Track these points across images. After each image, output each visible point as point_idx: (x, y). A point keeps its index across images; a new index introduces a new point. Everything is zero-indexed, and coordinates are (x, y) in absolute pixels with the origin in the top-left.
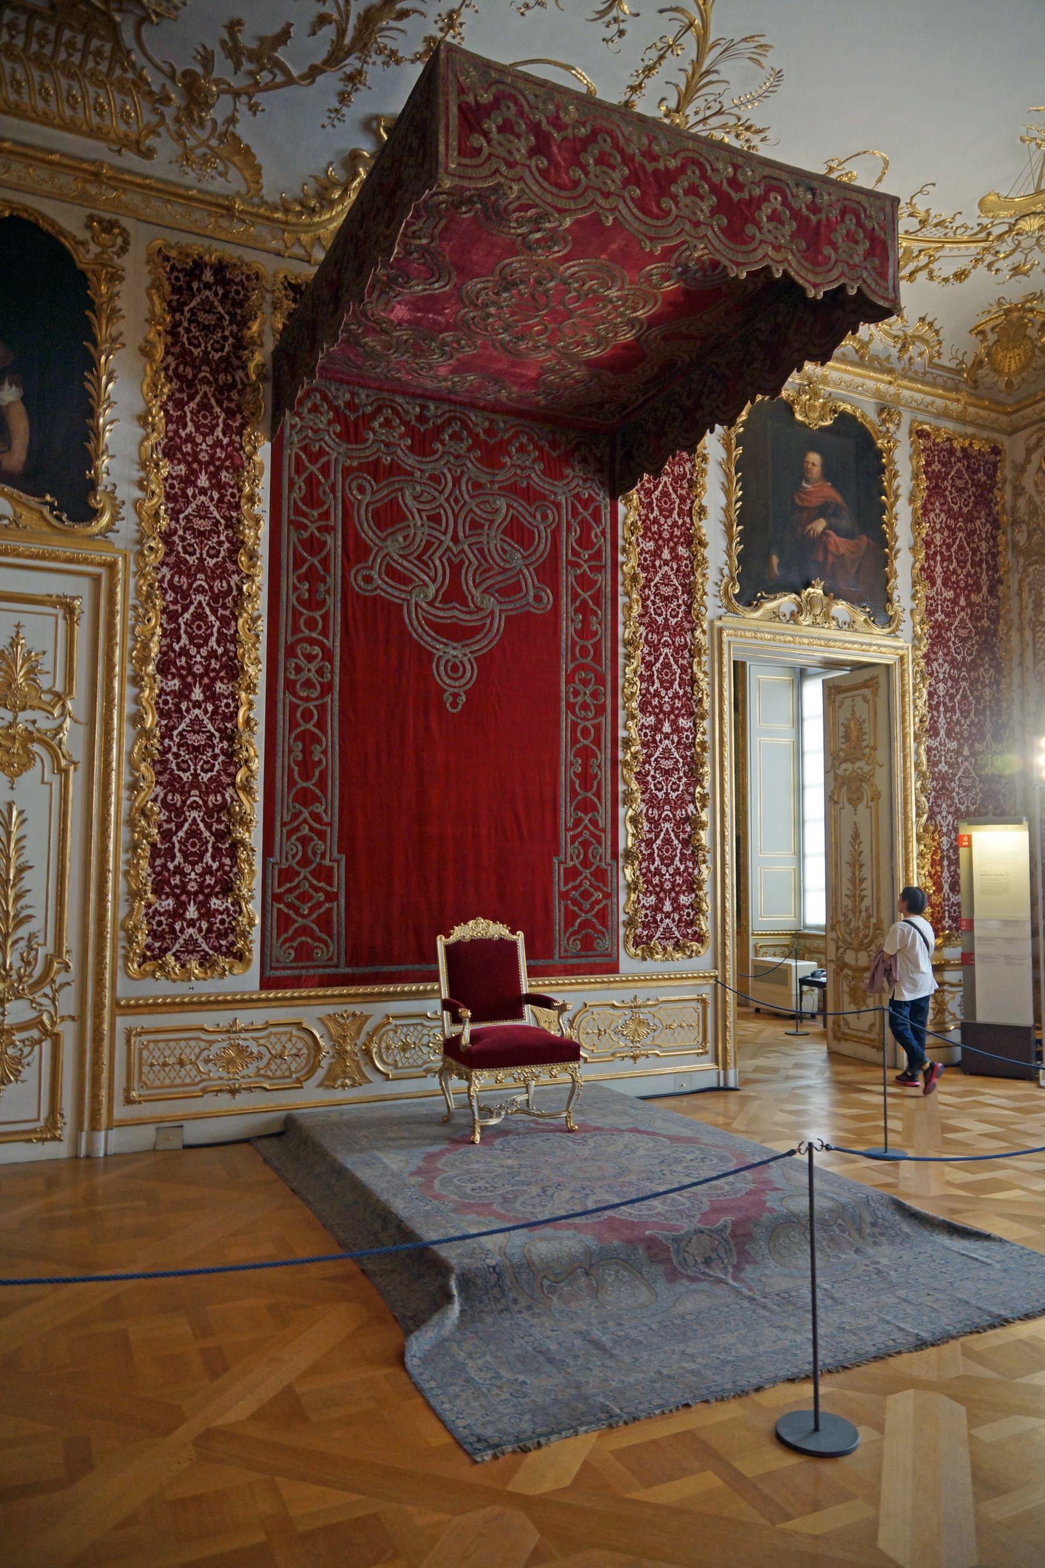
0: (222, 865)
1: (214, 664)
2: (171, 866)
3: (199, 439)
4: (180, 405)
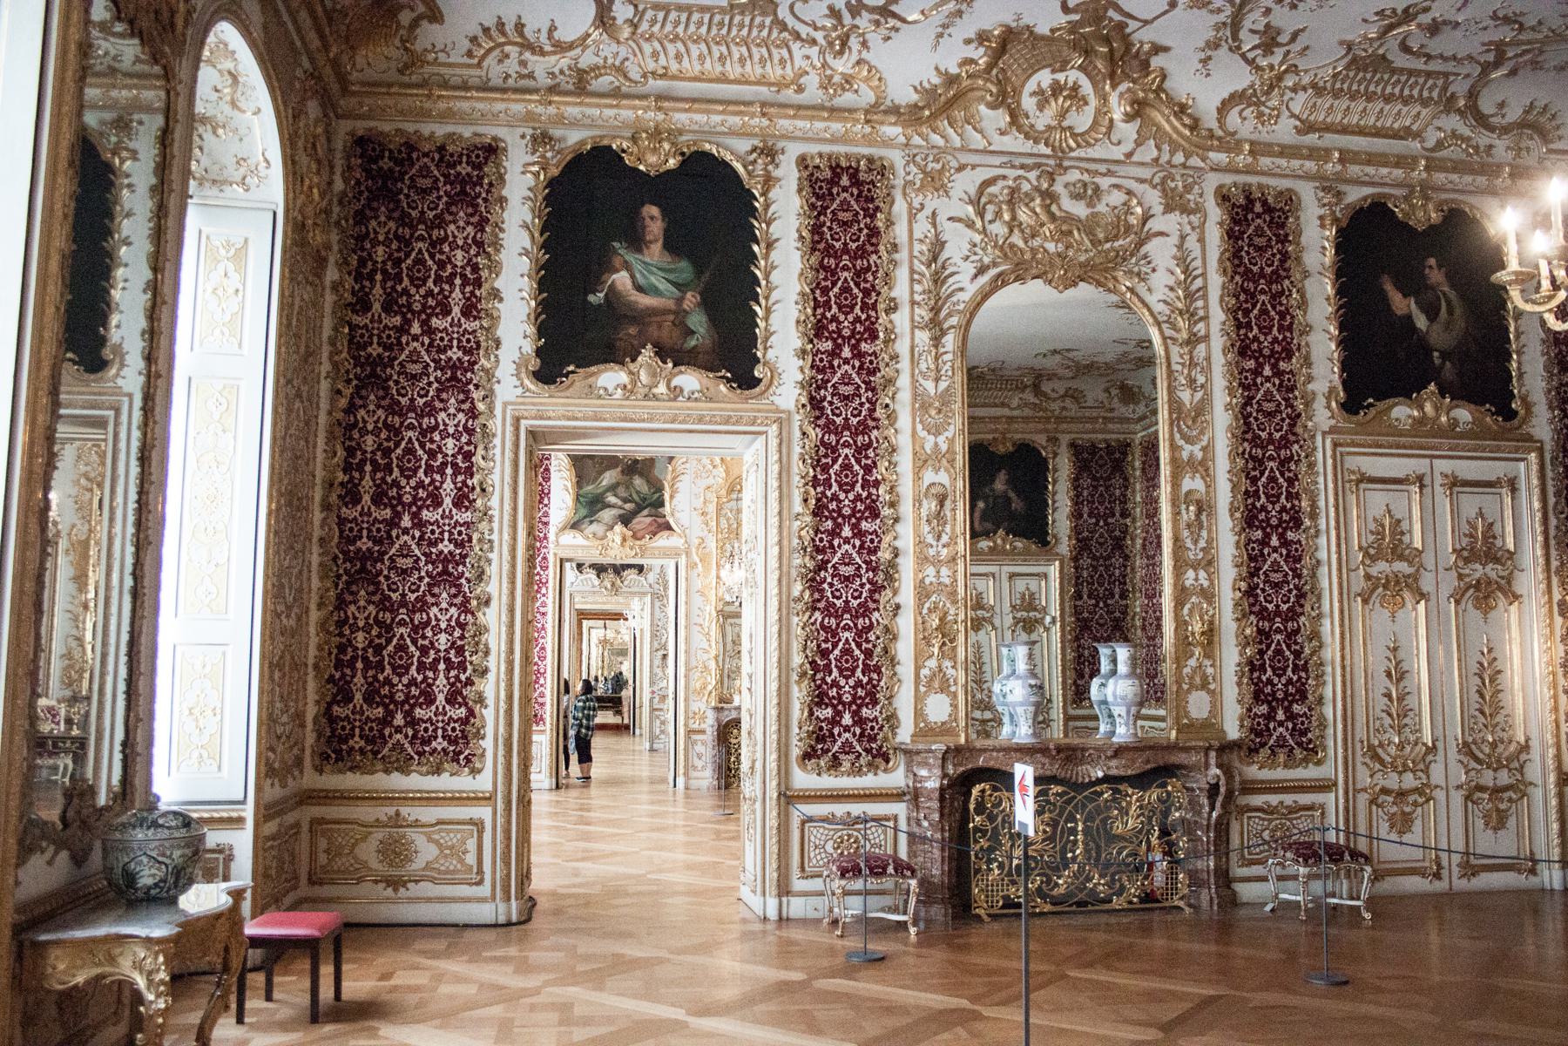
0: (871, 680)
1: (860, 506)
2: (829, 680)
3: (842, 318)
4: (825, 291)
